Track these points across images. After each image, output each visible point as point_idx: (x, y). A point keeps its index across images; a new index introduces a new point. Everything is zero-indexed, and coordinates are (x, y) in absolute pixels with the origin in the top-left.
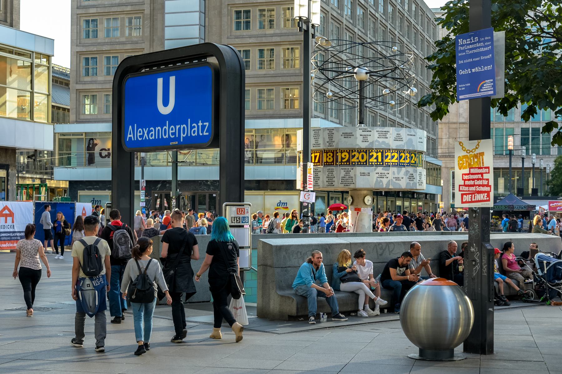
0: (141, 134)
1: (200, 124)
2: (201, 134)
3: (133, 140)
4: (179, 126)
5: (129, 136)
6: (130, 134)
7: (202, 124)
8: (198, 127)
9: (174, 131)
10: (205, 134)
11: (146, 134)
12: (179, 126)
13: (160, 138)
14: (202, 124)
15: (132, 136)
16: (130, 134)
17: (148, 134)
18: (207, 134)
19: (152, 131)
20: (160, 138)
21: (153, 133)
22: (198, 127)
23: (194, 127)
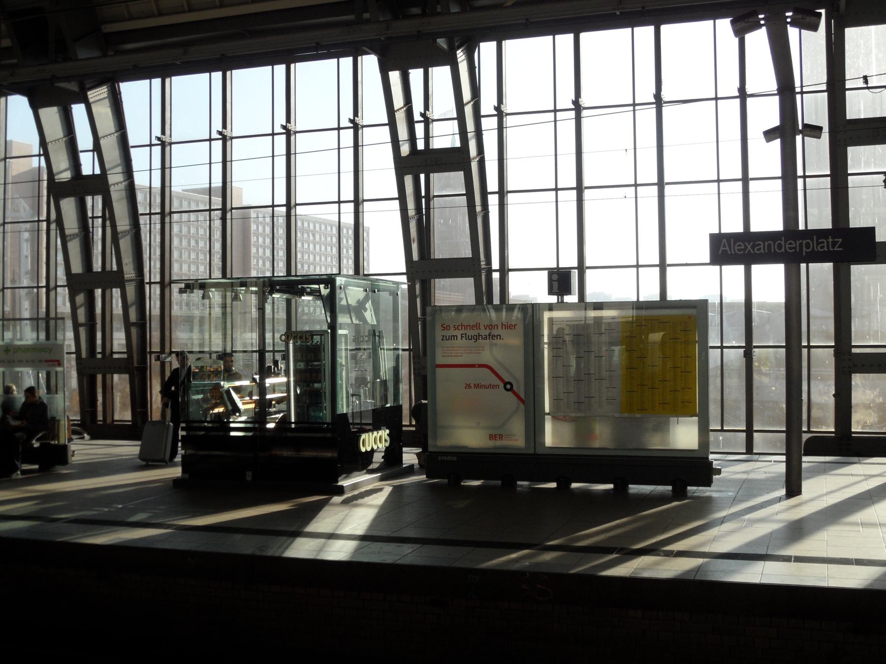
0: (743, 247)
1: (830, 240)
2: (832, 249)
3: (729, 253)
4: (801, 241)
5: (722, 248)
6: (724, 246)
7: (832, 240)
8: (828, 242)
9: (794, 246)
10: (836, 249)
11: (749, 247)
12: (801, 241)
13: (773, 251)
14: (832, 240)
15: (727, 248)
16: (724, 246)
17: (753, 247)
18: (841, 249)
19: (760, 245)
20: (773, 251)
21: (762, 247)
22: (828, 242)
23: (823, 242)
